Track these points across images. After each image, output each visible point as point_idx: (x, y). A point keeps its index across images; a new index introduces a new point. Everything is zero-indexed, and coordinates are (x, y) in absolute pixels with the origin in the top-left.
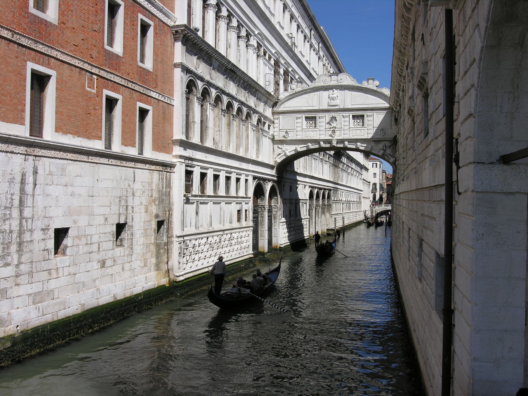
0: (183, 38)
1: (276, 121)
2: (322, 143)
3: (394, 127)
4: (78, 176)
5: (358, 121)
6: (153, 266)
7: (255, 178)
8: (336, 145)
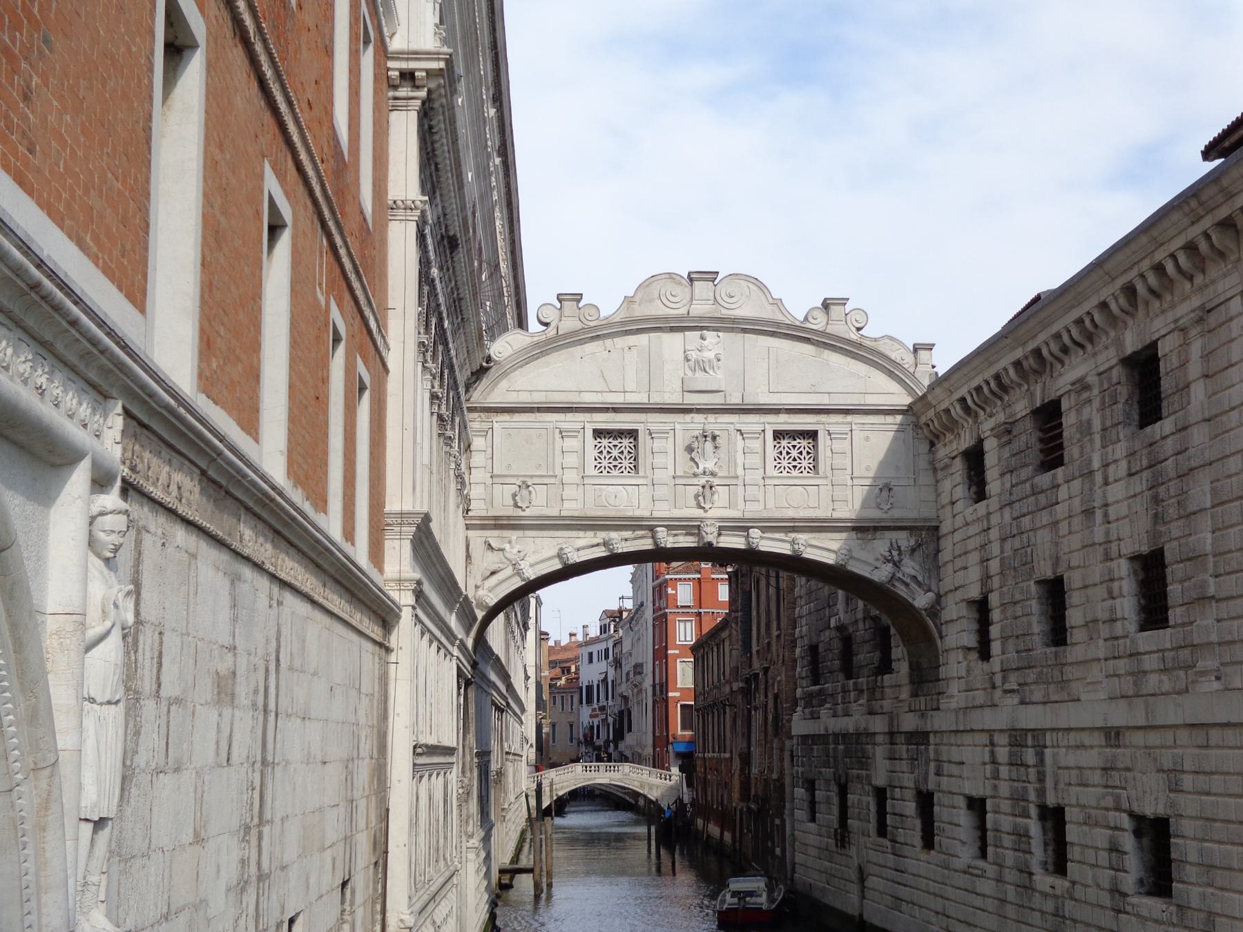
0: (423, 103)
1: (478, 443)
2: (661, 533)
3: (926, 479)
4: (315, 674)
5: (794, 453)
7: (458, 668)
8: (715, 544)
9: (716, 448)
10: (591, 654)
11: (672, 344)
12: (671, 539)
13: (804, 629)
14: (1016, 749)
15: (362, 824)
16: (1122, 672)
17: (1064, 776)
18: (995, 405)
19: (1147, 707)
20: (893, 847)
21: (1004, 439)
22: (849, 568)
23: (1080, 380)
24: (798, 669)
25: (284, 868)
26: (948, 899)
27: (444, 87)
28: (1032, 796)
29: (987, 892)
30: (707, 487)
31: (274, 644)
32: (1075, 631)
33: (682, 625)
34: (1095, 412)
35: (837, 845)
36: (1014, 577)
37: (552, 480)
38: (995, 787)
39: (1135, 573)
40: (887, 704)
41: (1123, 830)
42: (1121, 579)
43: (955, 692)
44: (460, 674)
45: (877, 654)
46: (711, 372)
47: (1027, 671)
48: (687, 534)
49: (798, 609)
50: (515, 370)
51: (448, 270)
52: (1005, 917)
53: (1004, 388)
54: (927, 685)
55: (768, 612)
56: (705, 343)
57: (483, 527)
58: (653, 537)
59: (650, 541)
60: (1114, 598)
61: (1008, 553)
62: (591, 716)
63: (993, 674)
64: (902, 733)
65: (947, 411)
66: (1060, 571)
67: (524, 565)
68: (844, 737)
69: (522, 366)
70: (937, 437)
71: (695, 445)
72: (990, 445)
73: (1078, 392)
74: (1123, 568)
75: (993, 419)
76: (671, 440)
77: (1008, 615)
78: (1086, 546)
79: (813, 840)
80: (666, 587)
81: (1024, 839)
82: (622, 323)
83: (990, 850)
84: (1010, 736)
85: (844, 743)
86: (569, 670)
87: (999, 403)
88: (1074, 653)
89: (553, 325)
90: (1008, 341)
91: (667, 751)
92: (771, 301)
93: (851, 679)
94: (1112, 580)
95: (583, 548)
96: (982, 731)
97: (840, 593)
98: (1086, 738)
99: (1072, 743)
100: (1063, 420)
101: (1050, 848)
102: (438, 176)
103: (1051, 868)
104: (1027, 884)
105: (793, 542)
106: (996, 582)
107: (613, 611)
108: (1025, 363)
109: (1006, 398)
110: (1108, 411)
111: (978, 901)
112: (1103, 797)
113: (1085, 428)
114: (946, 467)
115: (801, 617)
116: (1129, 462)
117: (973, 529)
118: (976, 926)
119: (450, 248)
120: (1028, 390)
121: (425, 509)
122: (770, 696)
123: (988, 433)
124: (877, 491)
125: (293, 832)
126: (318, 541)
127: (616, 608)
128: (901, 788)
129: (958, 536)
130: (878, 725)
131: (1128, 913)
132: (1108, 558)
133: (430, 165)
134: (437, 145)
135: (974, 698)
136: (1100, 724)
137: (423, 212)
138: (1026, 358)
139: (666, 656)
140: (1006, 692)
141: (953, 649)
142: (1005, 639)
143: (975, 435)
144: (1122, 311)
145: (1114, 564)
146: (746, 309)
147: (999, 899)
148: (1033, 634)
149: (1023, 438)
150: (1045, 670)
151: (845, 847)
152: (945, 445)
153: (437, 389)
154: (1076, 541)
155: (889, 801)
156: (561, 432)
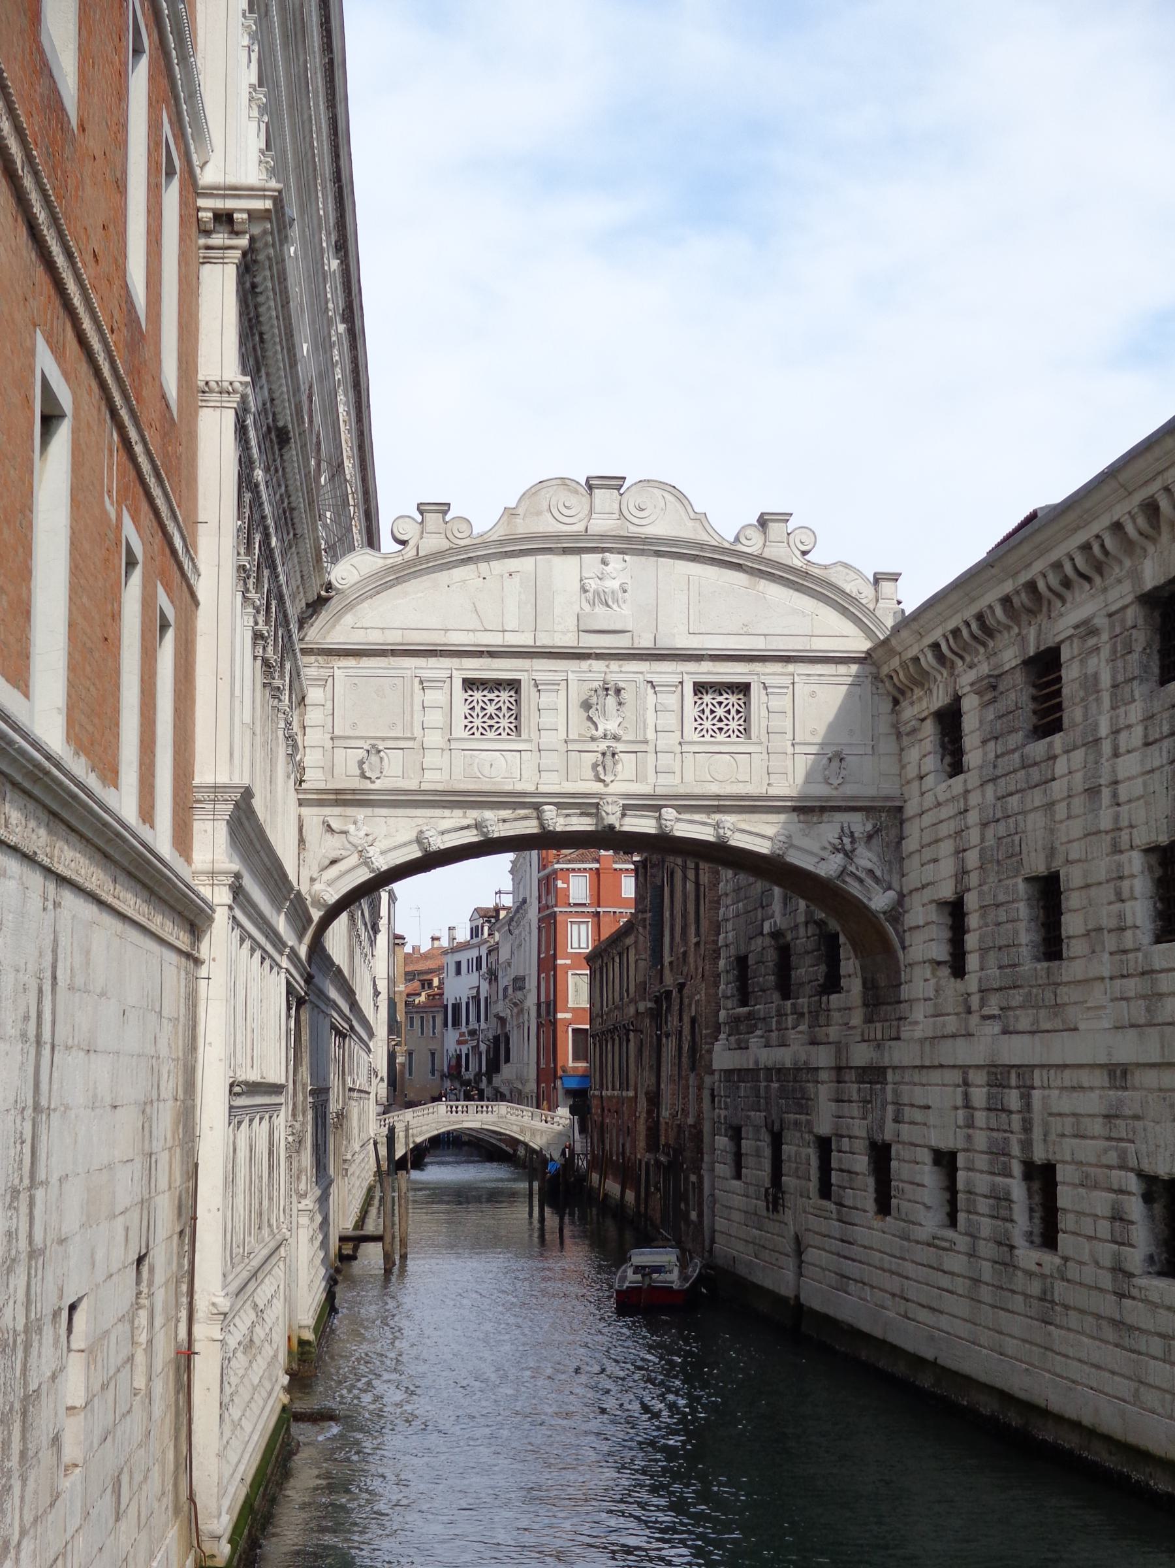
0: (244, 254)
1: (314, 695)
2: (549, 812)
3: (888, 745)
4: (103, 994)
5: (720, 712)
6: (171, 1487)
7: (288, 983)
8: (617, 826)
9: (620, 704)
10: (458, 964)
11: (566, 569)
12: (561, 821)
13: (730, 935)
14: (994, 1090)
15: (163, 1183)
16: (1132, 994)
17: (1056, 1125)
18: (977, 653)
19: (1162, 1037)
20: (839, 1212)
21: (989, 696)
22: (788, 859)
23: (1085, 622)
24: (722, 987)
25: (62, 1241)
26: (907, 1278)
27: (272, 233)
28: (1016, 1150)
29: (956, 1270)
30: (609, 754)
31: (49, 958)
32: (1073, 941)
33: (575, 927)
34: (1103, 664)
35: (768, 1209)
36: (998, 872)
37: (409, 744)
38: (969, 1138)
39: (1151, 869)
40: (833, 1032)
41: (1129, 1193)
42: (1133, 876)
43: (921, 1017)
44: (290, 990)
45: (823, 968)
46: (615, 607)
47: (1012, 992)
48: (582, 814)
49: (722, 911)
50: (363, 601)
51: (276, 471)
52: (979, 1301)
53: (989, 631)
54: (884, 1007)
55: (684, 915)
56: (608, 569)
57: (321, 803)
58: (538, 818)
59: (535, 823)
60: (1123, 901)
61: (990, 841)
62: (459, 1042)
63: (969, 995)
64: (851, 1068)
65: (916, 660)
66: (1057, 864)
67: (372, 852)
68: (778, 1072)
69: (371, 597)
70: (902, 693)
71: (594, 700)
72: (970, 704)
73: (1083, 638)
74: (1135, 862)
75: (974, 671)
76: (563, 693)
77: (989, 920)
78: (1089, 835)
79: (738, 1201)
80: (555, 879)
81: (1003, 1203)
82: (502, 542)
83: (961, 1217)
84: (988, 1073)
85: (778, 1081)
86: (430, 983)
87: (982, 650)
88: (1071, 970)
89: (412, 543)
90: (994, 571)
91: (555, 1088)
92: (692, 515)
93: (789, 999)
94: (1121, 878)
95: (449, 831)
96: (954, 1067)
97: (777, 891)
98: (1085, 1078)
99: (1067, 1083)
100: (1063, 673)
101: (1037, 1215)
102: (263, 350)
103: (1037, 1240)
104: (1008, 1260)
105: (717, 826)
106: (974, 879)
107: (488, 909)
108: (1016, 600)
109: (991, 644)
110: (1120, 663)
111: (945, 1281)
112: (1106, 1151)
113: (1091, 684)
114: (914, 731)
115: (727, 920)
116: (1146, 728)
117: (946, 811)
118: (941, 1312)
119: (279, 443)
120: (1019, 634)
121: (246, 782)
122: (686, 1019)
123: (967, 689)
124: (825, 761)
125: (75, 1195)
126: (106, 824)
127: (491, 905)
128: (850, 1137)
129: (927, 819)
130: (823, 1057)
131: (1134, 1298)
132: (1116, 850)
133: (253, 335)
134: (262, 310)
135: (944, 1025)
136: (1103, 1059)
137: (244, 398)
138: (1017, 592)
139: (555, 967)
140: (985, 1018)
141: (919, 963)
142: (984, 951)
143: (950, 690)
144: (1141, 534)
145: (1124, 858)
146: (660, 527)
147: (971, 1279)
148: (1020, 945)
149: (1012, 696)
150: (1034, 990)
151: (778, 1212)
152: (912, 704)
153: (261, 626)
154: (1076, 828)
155: (834, 1154)
156: (421, 682)
